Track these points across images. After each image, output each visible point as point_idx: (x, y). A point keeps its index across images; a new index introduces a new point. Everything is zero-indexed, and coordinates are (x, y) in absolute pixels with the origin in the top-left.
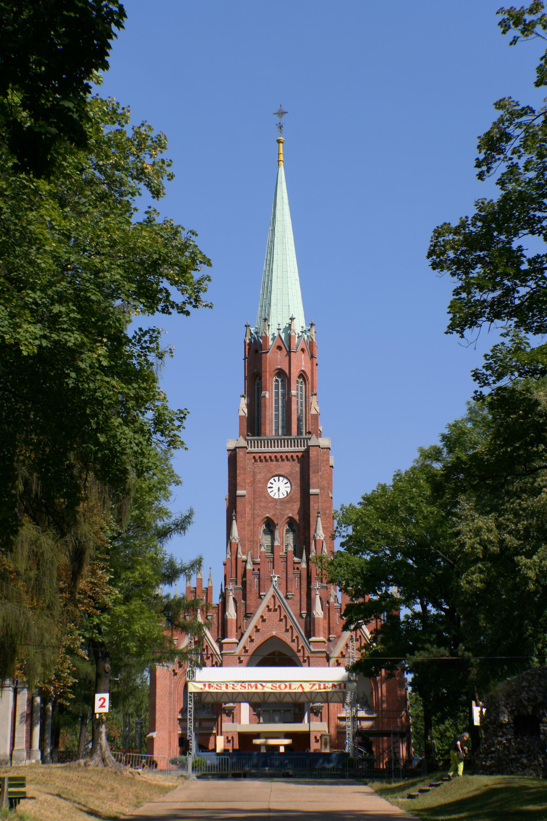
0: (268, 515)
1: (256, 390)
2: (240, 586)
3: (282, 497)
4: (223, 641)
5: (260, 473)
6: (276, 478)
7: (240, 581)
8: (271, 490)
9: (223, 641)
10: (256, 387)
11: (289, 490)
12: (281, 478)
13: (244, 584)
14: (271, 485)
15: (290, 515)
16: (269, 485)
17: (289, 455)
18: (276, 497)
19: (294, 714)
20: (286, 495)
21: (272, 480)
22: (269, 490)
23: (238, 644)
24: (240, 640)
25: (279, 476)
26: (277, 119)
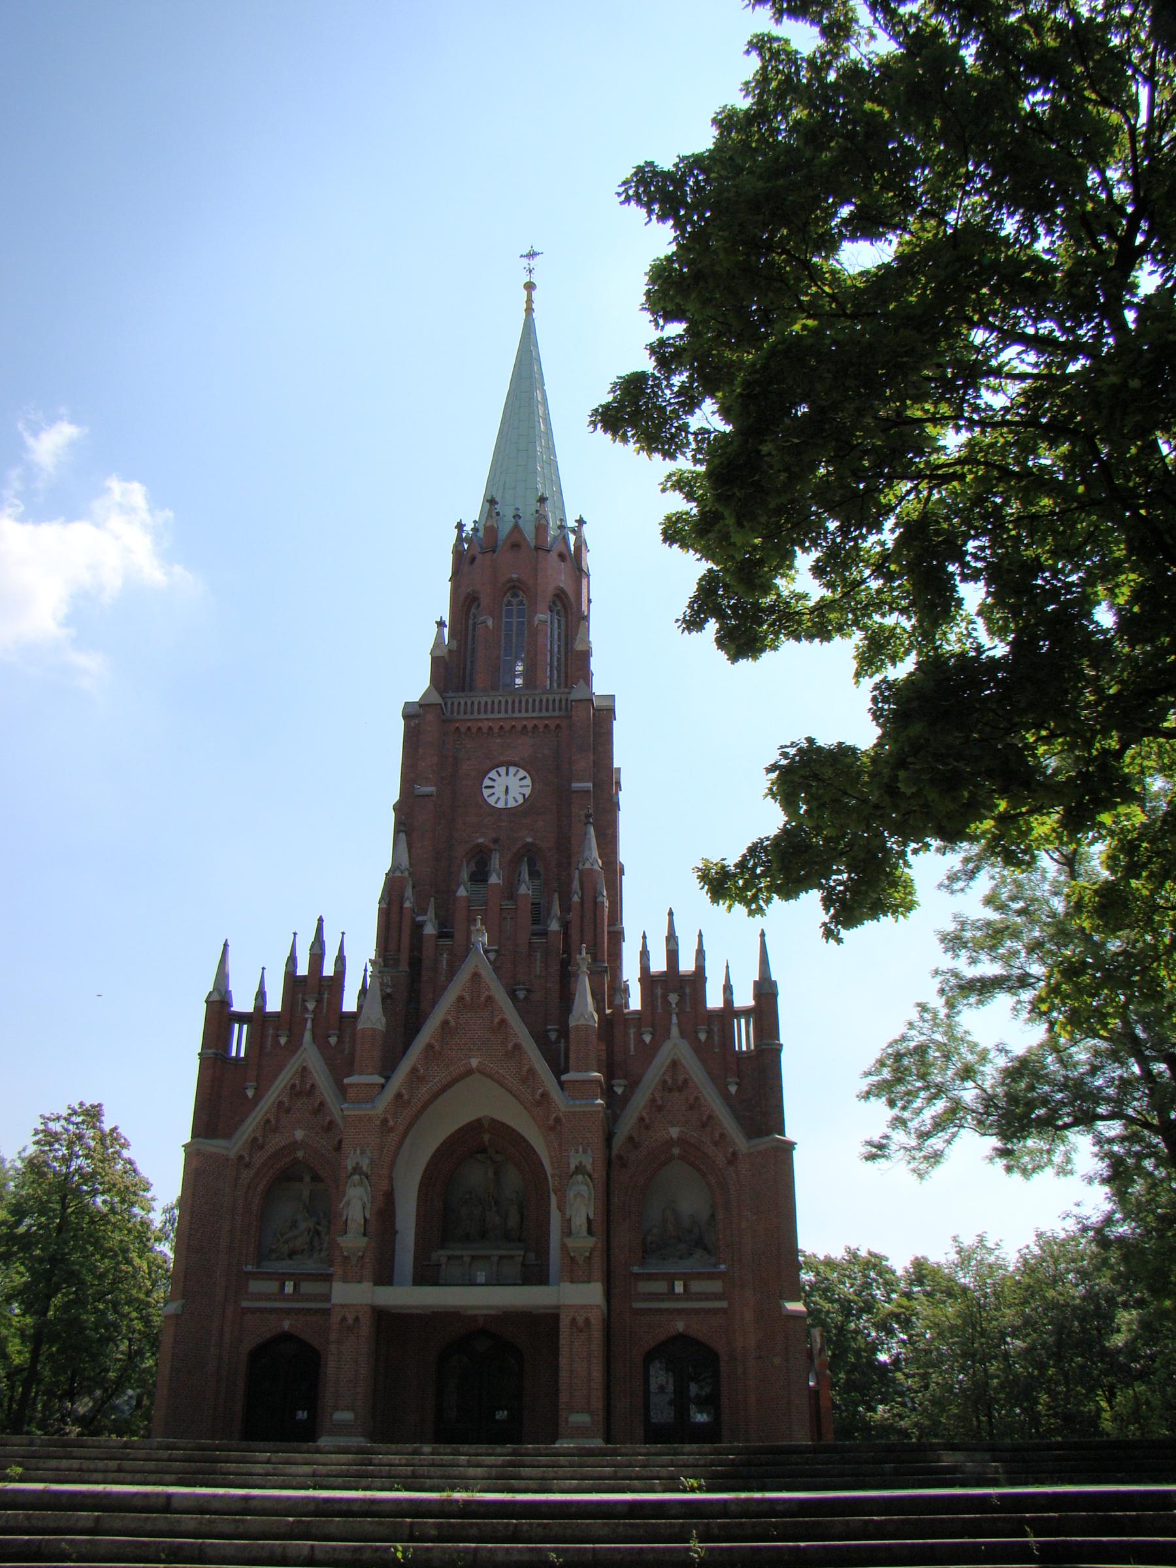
0: (481, 840)
1: (470, 627)
2: (404, 967)
3: (512, 804)
4: (346, 1081)
5: (469, 759)
6: (502, 770)
7: (405, 956)
8: (491, 791)
9: (346, 1081)
10: (471, 622)
11: (527, 791)
12: (512, 770)
13: (416, 964)
14: (491, 783)
15: (529, 840)
16: (487, 782)
17: (530, 725)
18: (501, 805)
19: (523, 1265)
20: (521, 801)
21: (493, 774)
22: (486, 792)
23: (383, 1086)
24: (387, 1078)
25: (508, 764)
26: (525, 261)
